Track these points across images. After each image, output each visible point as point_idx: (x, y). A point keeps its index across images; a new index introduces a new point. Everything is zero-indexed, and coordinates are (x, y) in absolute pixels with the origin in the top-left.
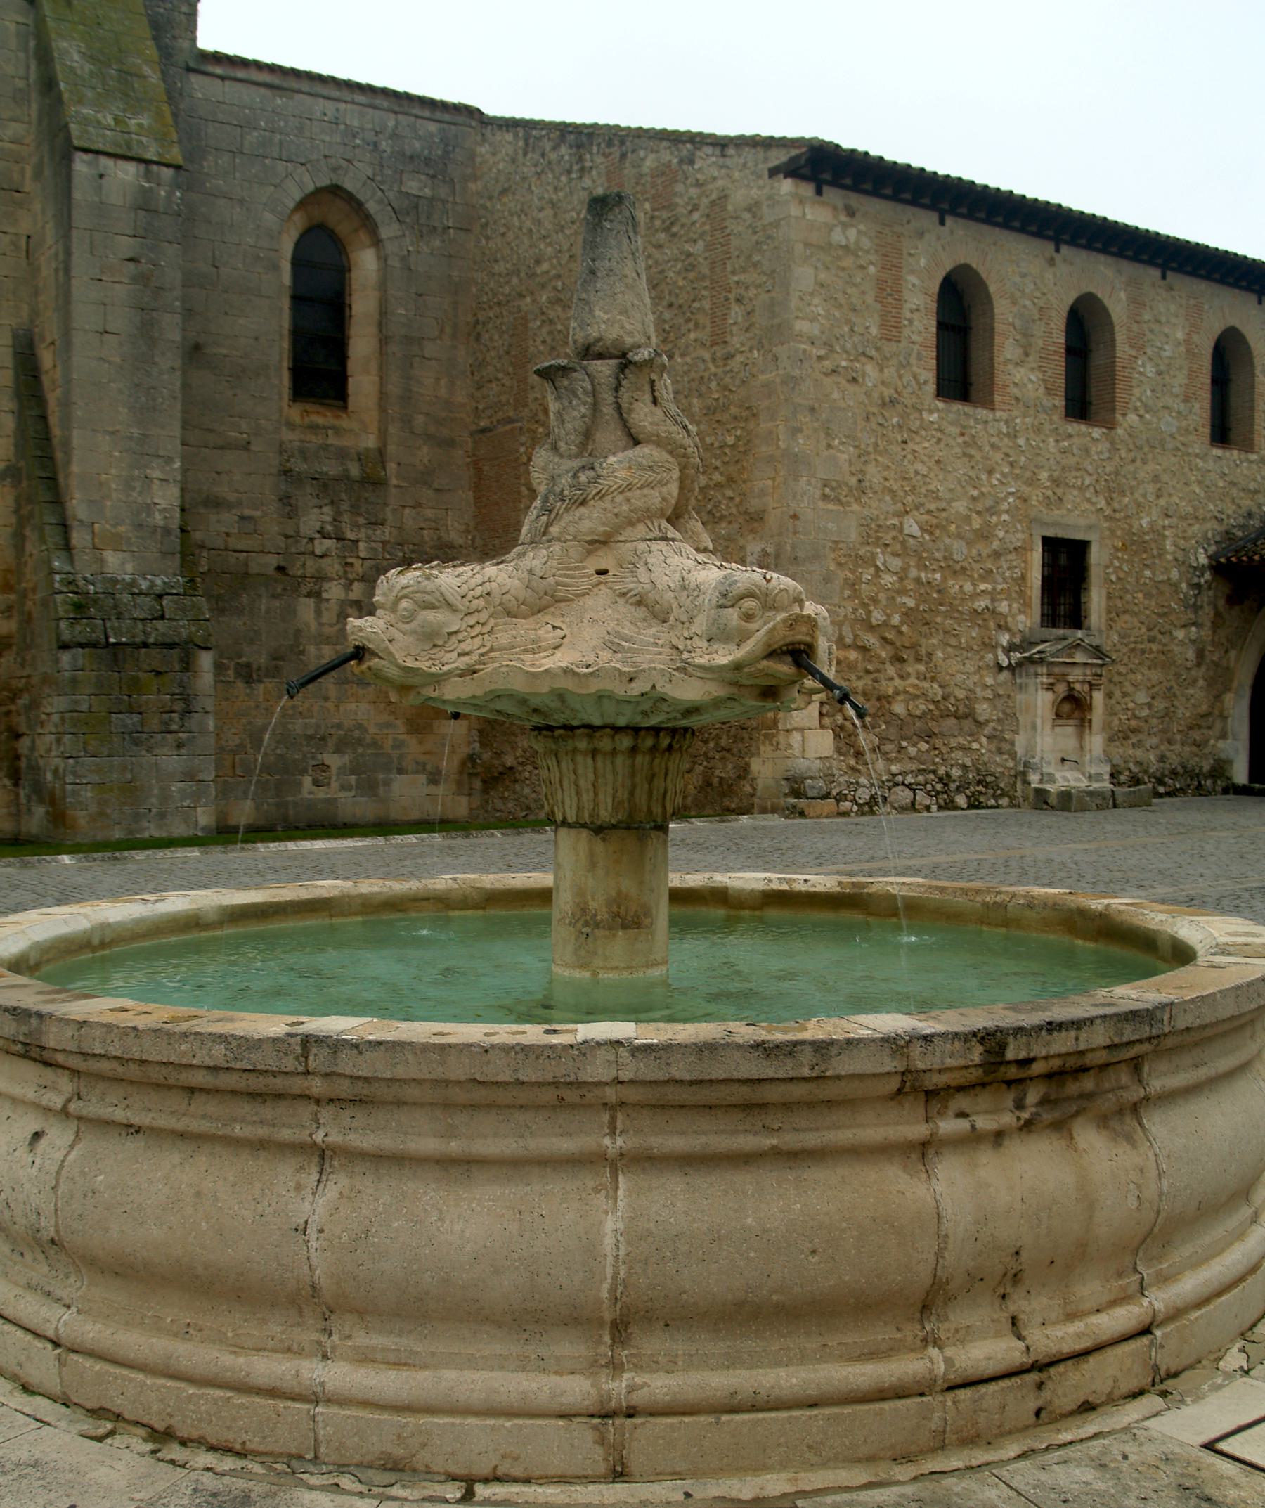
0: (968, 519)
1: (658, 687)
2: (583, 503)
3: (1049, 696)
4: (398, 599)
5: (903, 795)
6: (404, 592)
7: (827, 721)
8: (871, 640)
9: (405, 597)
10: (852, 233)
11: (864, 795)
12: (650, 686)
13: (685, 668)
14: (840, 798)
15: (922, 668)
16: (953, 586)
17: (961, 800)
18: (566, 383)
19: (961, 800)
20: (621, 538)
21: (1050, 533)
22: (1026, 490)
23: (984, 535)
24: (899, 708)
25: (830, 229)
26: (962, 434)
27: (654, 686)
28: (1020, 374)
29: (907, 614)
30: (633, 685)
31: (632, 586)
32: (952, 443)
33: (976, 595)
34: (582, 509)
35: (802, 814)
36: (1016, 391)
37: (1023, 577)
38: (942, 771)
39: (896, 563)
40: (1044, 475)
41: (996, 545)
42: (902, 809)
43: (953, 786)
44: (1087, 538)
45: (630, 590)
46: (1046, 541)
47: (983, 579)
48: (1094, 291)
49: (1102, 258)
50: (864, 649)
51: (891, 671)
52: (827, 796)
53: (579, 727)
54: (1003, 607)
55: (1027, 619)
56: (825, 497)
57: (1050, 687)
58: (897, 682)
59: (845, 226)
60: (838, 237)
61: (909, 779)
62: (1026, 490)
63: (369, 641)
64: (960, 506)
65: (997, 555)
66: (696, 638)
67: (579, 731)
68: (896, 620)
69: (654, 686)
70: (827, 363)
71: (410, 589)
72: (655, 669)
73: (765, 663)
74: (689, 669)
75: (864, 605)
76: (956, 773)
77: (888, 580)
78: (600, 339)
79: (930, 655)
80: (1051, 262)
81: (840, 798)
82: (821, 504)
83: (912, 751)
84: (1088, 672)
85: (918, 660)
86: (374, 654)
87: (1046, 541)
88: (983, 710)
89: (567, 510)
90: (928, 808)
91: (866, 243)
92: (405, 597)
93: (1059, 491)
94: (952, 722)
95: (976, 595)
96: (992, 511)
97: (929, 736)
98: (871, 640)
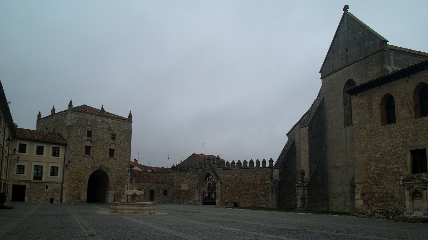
0: (391, 151)
3: (408, 192)
5: (377, 215)
7: (362, 198)
8: (370, 181)
10: (362, 100)
11: (369, 214)
14: (364, 214)
15: (382, 186)
16: (388, 167)
17: (391, 217)
19: (391, 217)
21: (413, 149)
22: (405, 140)
23: (396, 153)
24: (376, 195)
25: (358, 101)
26: (389, 132)
28: (402, 112)
29: (377, 174)
32: (386, 134)
33: (393, 168)
35: (357, 216)
36: (401, 117)
37: (406, 162)
38: (387, 210)
39: (374, 164)
40: (410, 135)
41: (398, 155)
42: (377, 218)
43: (390, 214)
44: (425, 148)
46: (411, 151)
47: (395, 164)
48: (422, 81)
49: (423, 71)
50: (368, 183)
51: (375, 187)
52: (362, 213)
54: (401, 170)
55: (407, 172)
56: (360, 154)
57: (409, 189)
58: (377, 189)
59: (361, 99)
60: (360, 102)
61: (379, 211)
62: (405, 140)
64: (389, 148)
65: (399, 158)
68: (375, 176)
70: (359, 128)
75: (368, 174)
76: (390, 211)
77: (373, 168)
79: (383, 183)
80: (407, 81)
81: (364, 214)
82: (359, 155)
83: (379, 205)
84: (421, 185)
85: (381, 185)
87: (411, 151)
88: (397, 196)
90: (383, 218)
91: (365, 100)
93: (416, 138)
94: (389, 198)
95: (393, 168)
96: (398, 147)
97: (384, 202)
98: (370, 181)
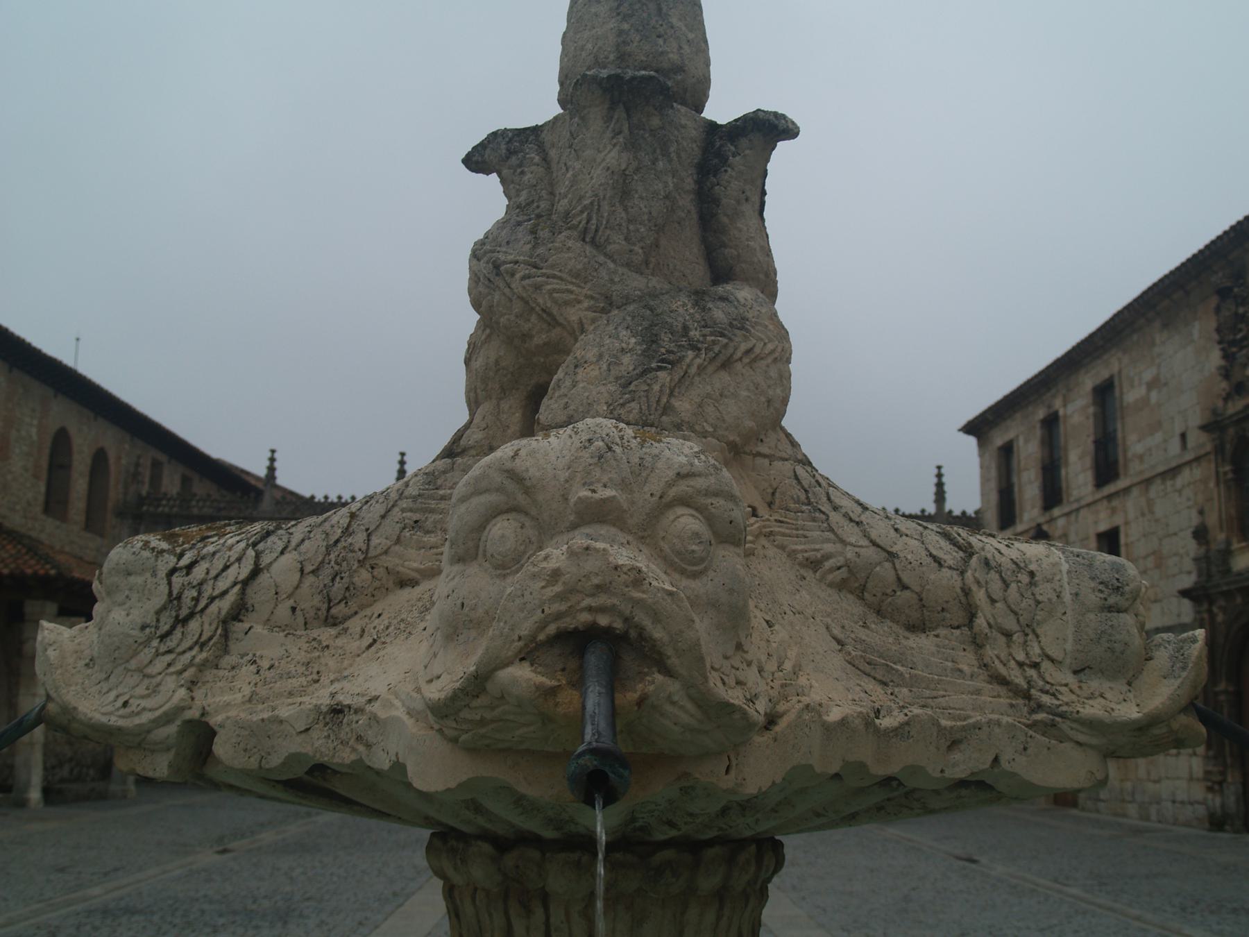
1: (1005, 765)
2: (726, 365)
4: (665, 505)
6: (682, 487)
9: (684, 501)
12: (991, 758)
13: (1053, 725)
18: (656, 122)
20: (764, 449)
27: (996, 760)
30: (956, 756)
31: (828, 548)
34: (724, 376)
45: (827, 557)
53: (710, 843)
63: (656, 617)
66: (1046, 665)
67: (711, 852)
69: (996, 760)
71: (700, 483)
72: (999, 723)
73: (1184, 719)
74: (1065, 726)
78: (680, 69)
86: (655, 659)
89: (701, 369)
92: (684, 501)
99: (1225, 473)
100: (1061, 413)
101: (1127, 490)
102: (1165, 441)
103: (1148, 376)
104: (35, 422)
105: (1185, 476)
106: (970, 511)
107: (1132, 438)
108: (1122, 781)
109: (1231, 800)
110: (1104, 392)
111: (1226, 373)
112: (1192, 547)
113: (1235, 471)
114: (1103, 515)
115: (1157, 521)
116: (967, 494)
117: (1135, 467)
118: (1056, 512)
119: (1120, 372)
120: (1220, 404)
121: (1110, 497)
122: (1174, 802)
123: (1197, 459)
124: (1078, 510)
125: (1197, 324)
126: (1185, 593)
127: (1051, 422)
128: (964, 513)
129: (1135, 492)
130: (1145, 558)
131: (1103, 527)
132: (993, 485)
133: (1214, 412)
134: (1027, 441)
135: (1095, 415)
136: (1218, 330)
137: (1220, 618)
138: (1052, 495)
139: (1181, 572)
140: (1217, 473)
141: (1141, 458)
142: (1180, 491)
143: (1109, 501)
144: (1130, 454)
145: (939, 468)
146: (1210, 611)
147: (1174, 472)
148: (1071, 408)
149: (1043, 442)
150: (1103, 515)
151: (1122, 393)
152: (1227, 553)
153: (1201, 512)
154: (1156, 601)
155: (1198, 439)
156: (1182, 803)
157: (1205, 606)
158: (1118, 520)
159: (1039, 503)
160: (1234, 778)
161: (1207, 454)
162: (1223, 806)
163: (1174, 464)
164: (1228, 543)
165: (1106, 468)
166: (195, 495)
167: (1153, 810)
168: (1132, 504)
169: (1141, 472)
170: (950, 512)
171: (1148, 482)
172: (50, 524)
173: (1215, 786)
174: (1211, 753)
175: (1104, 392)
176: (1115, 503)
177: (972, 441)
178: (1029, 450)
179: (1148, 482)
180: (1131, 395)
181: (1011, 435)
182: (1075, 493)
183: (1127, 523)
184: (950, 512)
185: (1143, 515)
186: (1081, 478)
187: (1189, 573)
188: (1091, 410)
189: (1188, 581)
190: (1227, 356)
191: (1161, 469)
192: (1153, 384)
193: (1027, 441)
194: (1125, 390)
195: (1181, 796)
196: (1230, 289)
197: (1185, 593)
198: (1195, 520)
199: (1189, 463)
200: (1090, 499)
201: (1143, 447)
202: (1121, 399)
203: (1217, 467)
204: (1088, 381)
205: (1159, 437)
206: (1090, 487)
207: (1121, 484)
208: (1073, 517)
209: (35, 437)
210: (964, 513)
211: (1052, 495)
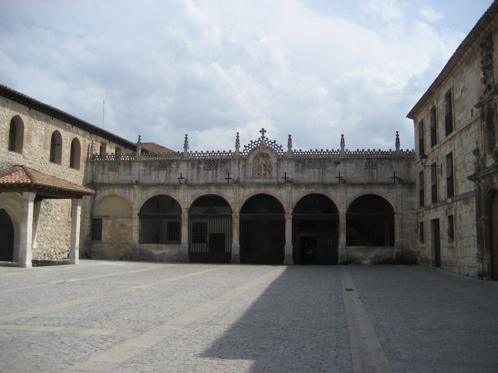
99: (484, 125)
100: (436, 106)
101: (455, 136)
102: (467, 114)
103: (461, 87)
104: (43, 128)
105: (473, 128)
106: (410, 150)
107: (457, 114)
108: (453, 258)
109: (486, 267)
110: (449, 96)
111: (485, 81)
112: (473, 158)
113: (487, 124)
114: (448, 147)
115: (464, 148)
116: (409, 143)
117: (458, 126)
118: (435, 147)
119: (453, 86)
120: (483, 95)
121: (450, 139)
122: (468, 266)
123: (476, 120)
124: (441, 145)
125: (476, 61)
126: (470, 178)
127: (434, 111)
128: (407, 150)
129: (457, 136)
130: (460, 164)
131: (448, 153)
132: (418, 138)
133: (481, 98)
134: (427, 119)
135: (446, 106)
136: (482, 62)
137: (482, 188)
138: (434, 141)
139: (471, 170)
140: (481, 125)
141: (459, 122)
142: (470, 135)
143: (450, 142)
144: (456, 121)
145: (397, 132)
146: (478, 185)
147: (468, 127)
148: (439, 104)
149: (431, 119)
150: (448, 147)
151: (453, 95)
152: (484, 160)
153: (477, 143)
154: (463, 182)
155: (477, 111)
156: (471, 267)
157: (477, 183)
158: (452, 149)
159: (430, 144)
160: (487, 257)
161: (479, 117)
162: (483, 268)
163: (469, 124)
164: (485, 155)
165: (449, 129)
166: (107, 154)
167: (462, 269)
168: (457, 141)
169: (459, 128)
170: (402, 150)
171: (461, 132)
172: (53, 165)
173: (481, 258)
174: (479, 246)
175: (449, 96)
176: (452, 142)
177: (412, 121)
178: (428, 123)
179: (461, 132)
180: (456, 96)
181: (423, 117)
182: (440, 139)
183: (455, 150)
184: (402, 150)
185: (460, 146)
186: (442, 132)
187: (473, 169)
188: (445, 104)
189: (472, 173)
190: (485, 74)
191: (465, 126)
192: (463, 90)
193: (427, 119)
194: (455, 94)
195: (470, 265)
196: (485, 43)
197: (470, 178)
198: (475, 146)
199: (473, 122)
200: (444, 141)
201: (462, 117)
202: (453, 97)
203: (481, 123)
204: (444, 91)
205: (465, 112)
206: (445, 136)
207: (453, 133)
208: (439, 149)
209: (43, 134)
210: (407, 150)
211: (434, 141)
